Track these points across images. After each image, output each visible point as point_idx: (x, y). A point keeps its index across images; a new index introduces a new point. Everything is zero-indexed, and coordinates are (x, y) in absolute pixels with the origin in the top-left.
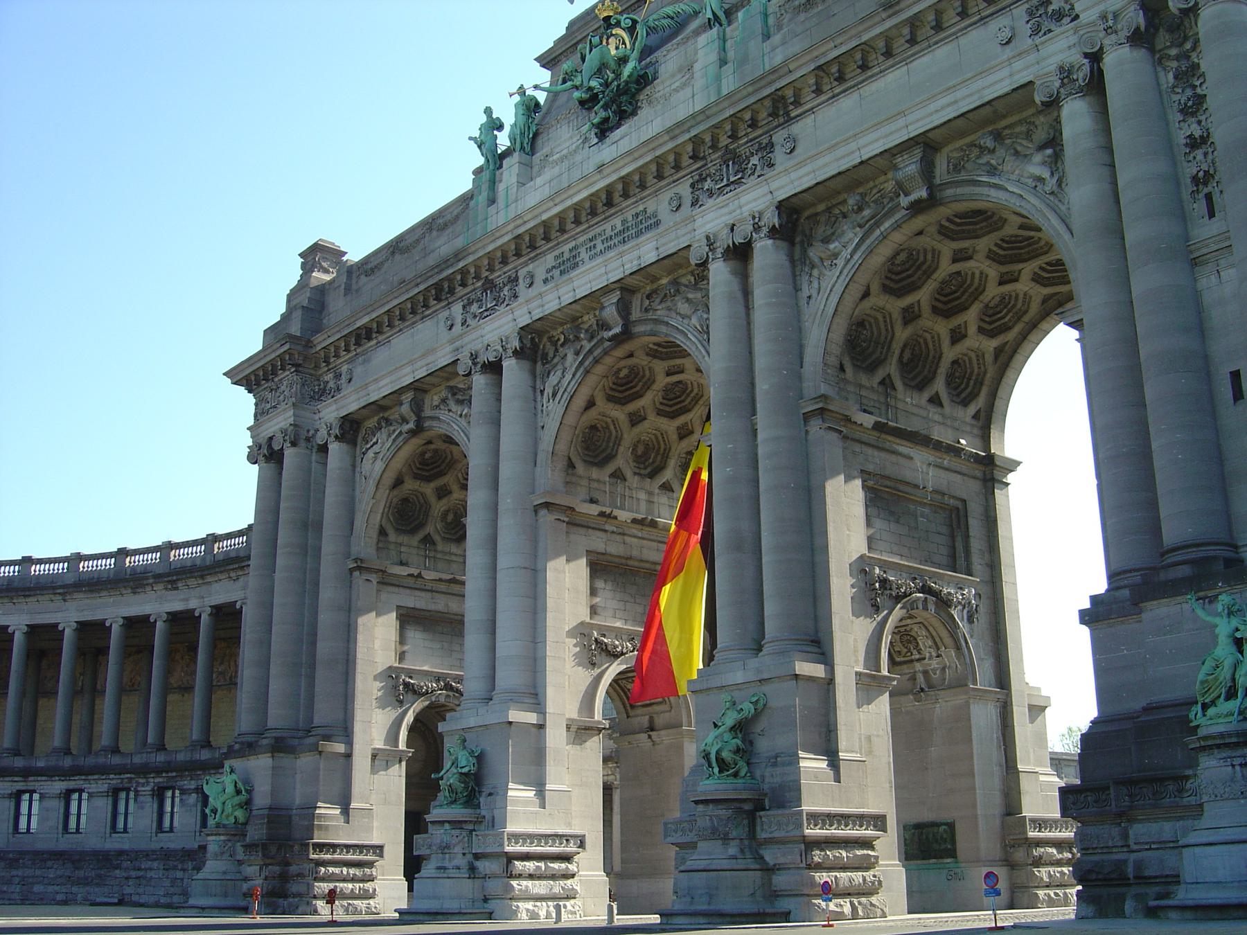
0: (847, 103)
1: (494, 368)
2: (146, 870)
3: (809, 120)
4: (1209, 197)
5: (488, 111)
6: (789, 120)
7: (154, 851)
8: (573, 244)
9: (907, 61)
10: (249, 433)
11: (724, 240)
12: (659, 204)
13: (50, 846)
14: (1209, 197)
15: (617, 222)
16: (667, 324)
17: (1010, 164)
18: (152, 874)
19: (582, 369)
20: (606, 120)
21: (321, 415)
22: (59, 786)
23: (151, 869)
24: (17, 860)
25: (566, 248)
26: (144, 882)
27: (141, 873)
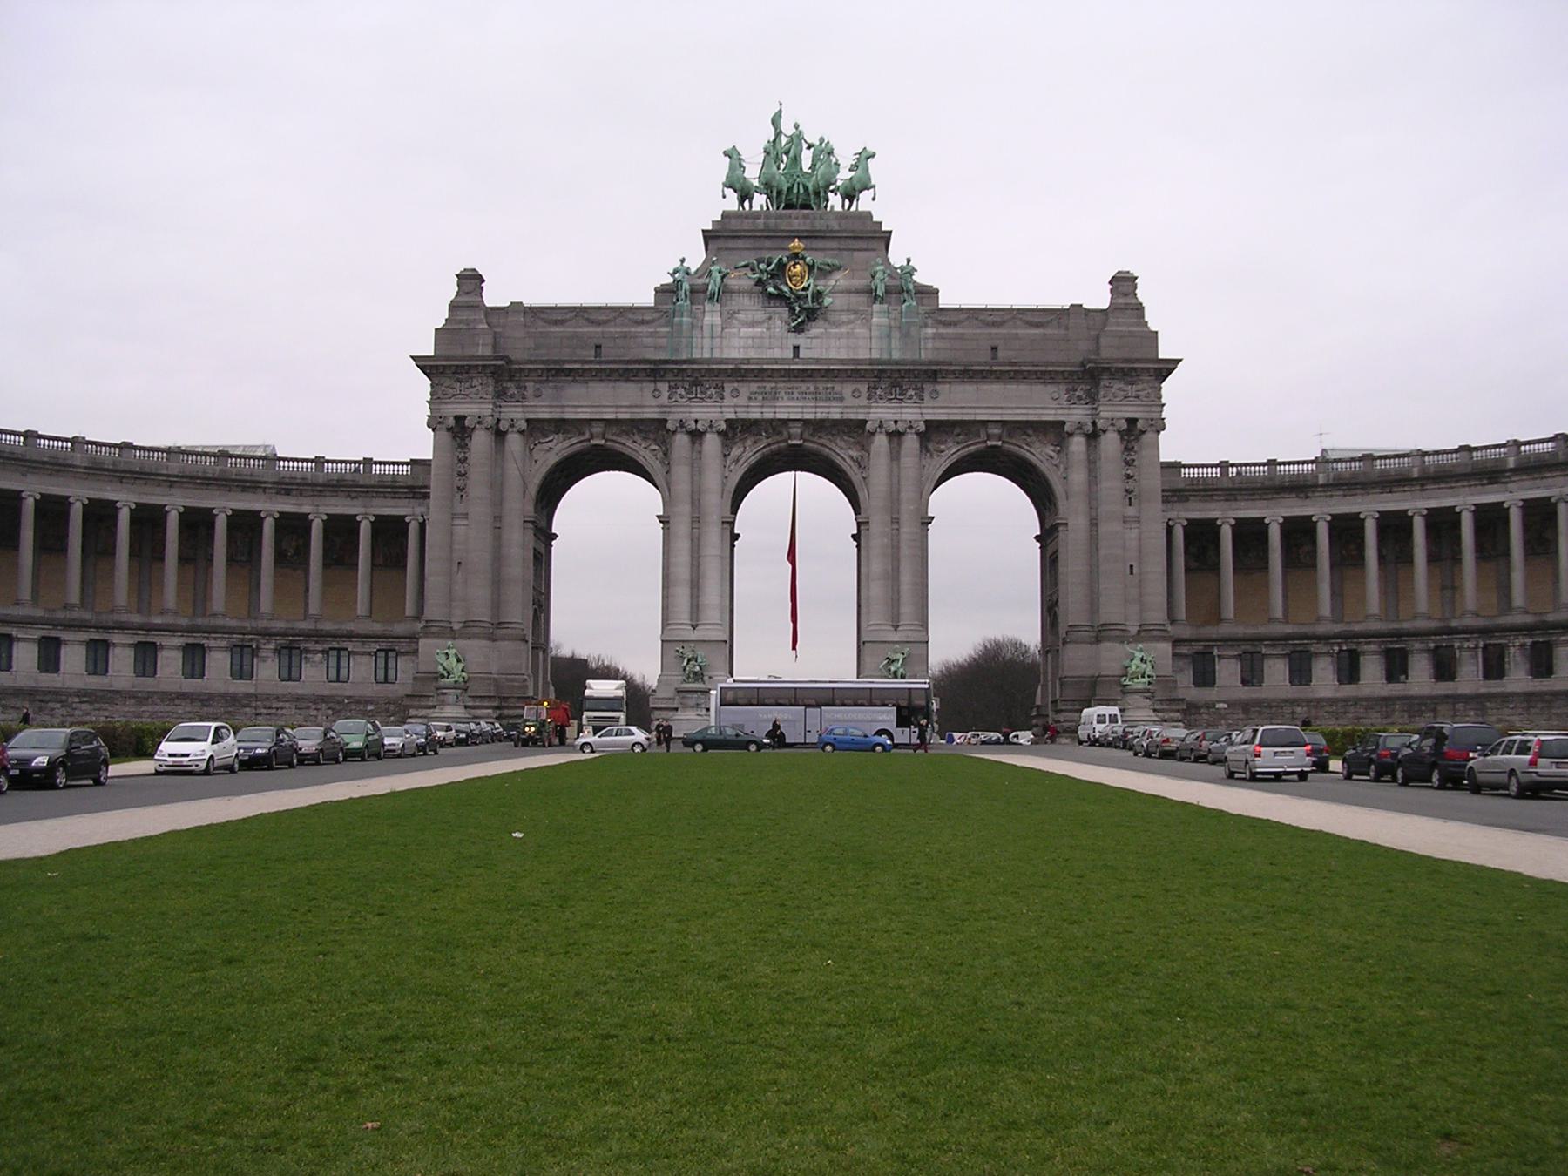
1: (696, 436)
2: (277, 709)
3: (947, 386)
4: (1130, 499)
5: (683, 261)
6: (935, 381)
7: (284, 696)
8: (774, 385)
9: (1005, 383)
11: (892, 427)
12: (847, 389)
13: (176, 688)
14: (1130, 499)
16: (831, 449)
17: (1037, 444)
18: (284, 711)
20: (803, 322)
21: (502, 410)
22: (178, 641)
23: (282, 708)
24: (147, 699)
25: (769, 386)
26: (273, 717)
27: (270, 711)
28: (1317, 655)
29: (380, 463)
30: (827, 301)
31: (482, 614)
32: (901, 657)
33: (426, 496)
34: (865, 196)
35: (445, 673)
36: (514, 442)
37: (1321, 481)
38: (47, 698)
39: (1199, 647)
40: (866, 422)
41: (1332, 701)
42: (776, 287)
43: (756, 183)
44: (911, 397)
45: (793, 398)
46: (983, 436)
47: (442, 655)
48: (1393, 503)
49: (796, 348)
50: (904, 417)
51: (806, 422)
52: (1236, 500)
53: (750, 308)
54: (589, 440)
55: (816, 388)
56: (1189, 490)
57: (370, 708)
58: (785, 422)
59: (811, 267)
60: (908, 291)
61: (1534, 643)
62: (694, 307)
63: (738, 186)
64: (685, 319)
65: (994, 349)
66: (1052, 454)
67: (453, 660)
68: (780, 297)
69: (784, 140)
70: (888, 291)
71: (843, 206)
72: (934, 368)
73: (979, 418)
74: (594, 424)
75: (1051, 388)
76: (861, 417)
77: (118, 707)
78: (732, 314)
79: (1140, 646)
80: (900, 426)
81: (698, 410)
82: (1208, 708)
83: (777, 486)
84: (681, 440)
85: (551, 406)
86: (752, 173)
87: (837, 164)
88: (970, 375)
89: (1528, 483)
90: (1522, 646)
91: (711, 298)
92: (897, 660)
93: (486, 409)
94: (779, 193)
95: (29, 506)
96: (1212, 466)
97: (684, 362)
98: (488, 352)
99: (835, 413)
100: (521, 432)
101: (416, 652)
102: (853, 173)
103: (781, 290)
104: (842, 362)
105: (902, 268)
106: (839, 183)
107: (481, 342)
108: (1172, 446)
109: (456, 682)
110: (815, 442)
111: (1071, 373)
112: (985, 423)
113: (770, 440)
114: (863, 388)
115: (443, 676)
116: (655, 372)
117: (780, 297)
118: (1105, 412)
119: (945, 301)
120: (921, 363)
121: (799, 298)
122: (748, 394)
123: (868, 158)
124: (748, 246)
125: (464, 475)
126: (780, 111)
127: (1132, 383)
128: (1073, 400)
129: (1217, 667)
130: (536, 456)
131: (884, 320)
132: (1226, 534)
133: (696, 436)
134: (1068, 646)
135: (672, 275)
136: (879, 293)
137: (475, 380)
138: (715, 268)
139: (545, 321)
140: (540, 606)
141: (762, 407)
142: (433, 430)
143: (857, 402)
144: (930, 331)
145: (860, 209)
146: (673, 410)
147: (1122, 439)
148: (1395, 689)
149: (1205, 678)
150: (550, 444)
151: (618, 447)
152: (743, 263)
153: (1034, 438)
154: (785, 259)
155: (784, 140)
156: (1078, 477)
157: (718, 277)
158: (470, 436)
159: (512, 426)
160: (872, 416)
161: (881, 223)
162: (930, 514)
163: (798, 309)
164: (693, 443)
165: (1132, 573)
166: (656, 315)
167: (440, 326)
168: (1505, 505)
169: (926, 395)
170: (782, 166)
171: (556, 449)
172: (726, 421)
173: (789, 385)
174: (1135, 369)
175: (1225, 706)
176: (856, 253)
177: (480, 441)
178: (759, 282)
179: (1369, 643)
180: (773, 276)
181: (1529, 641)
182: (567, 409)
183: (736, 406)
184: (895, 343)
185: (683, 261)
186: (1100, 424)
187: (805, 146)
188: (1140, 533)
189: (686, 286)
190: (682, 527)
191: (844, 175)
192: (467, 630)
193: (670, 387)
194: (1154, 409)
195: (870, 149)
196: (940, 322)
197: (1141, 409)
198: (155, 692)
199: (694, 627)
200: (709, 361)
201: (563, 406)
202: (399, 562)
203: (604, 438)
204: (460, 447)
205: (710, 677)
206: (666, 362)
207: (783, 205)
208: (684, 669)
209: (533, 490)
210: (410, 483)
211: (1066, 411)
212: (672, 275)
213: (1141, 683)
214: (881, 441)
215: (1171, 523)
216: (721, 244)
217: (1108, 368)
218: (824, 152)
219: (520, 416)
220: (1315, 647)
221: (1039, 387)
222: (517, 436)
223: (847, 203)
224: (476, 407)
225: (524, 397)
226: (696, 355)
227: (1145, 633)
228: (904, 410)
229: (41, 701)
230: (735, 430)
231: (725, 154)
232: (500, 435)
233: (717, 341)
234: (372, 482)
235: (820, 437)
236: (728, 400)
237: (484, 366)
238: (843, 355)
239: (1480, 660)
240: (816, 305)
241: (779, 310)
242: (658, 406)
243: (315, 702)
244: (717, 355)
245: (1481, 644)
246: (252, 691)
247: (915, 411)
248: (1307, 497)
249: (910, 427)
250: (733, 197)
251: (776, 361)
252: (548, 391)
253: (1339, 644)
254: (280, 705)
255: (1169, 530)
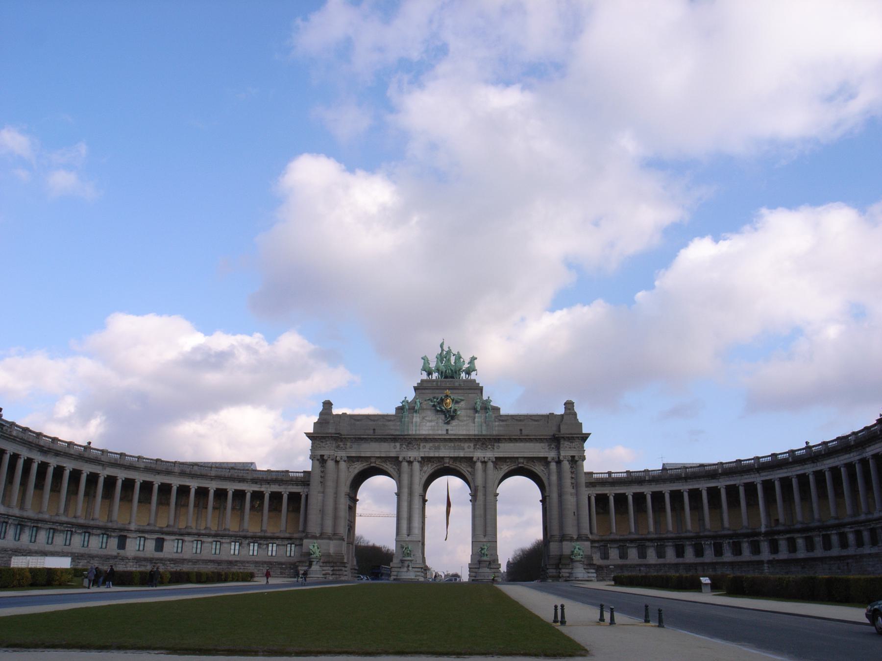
0: (512, 445)
1: (410, 463)
3: (503, 444)
5: (406, 398)
6: (499, 442)
7: (250, 561)
10: (310, 451)
11: (483, 460)
12: (466, 445)
15: (453, 445)
17: (537, 466)
18: (250, 568)
19: (433, 470)
20: (450, 420)
22: (210, 540)
23: (249, 566)
25: (437, 444)
27: (245, 567)
28: (648, 546)
29: (292, 472)
30: (459, 413)
31: (329, 530)
32: (486, 547)
33: (308, 485)
34: (473, 373)
35: (313, 553)
36: (343, 465)
37: (647, 479)
38: (157, 562)
39: (602, 544)
40: (472, 458)
41: (655, 565)
42: (440, 408)
43: (433, 369)
44: (489, 448)
45: (446, 449)
46: (517, 463)
47: (314, 547)
48: (676, 487)
49: (447, 430)
50: (487, 456)
51: (451, 458)
52: (614, 486)
53: (430, 415)
54: (370, 464)
55: (454, 445)
56: (596, 483)
57: (284, 566)
58: (443, 458)
59: (453, 400)
60: (489, 409)
61: (733, 542)
62: (410, 415)
63: (427, 370)
64: (406, 419)
65: (521, 430)
66: (543, 469)
67: (316, 548)
68: (442, 411)
69: (445, 353)
70: (481, 409)
71: (466, 377)
72: (498, 437)
73: (515, 456)
74: (372, 458)
75: (542, 444)
76: (471, 456)
77: (184, 566)
78: (423, 418)
79: (578, 543)
80: (486, 459)
81: (411, 453)
82: (606, 568)
83: (441, 483)
84: (405, 464)
85: (356, 452)
86: (433, 365)
87: (464, 361)
88: (511, 440)
89: (727, 479)
90: (729, 543)
91: (416, 412)
92: (485, 549)
93: (332, 453)
94: (442, 372)
95: (156, 487)
96: (605, 473)
97: (405, 435)
98: (333, 431)
99: (462, 455)
100: (345, 461)
101: (301, 545)
102: (469, 365)
103: (442, 409)
104: (463, 435)
105: (486, 400)
106: (464, 369)
107: (330, 428)
108: (588, 466)
109: (317, 556)
110: (454, 465)
111: (549, 439)
112: (517, 458)
113: (438, 465)
114: (472, 445)
115: (312, 554)
116: (394, 439)
117: (442, 411)
118: (563, 453)
119: (502, 412)
120: (494, 436)
121: (448, 411)
122: (429, 447)
123: (474, 360)
124: (430, 392)
125: (323, 477)
126: (443, 342)
127: (572, 442)
128: (550, 448)
129: (609, 551)
130: (350, 470)
131: (480, 420)
132: (612, 499)
133: (410, 463)
134: (551, 543)
135: (402, 403)
136: (478, 410)
137: (328, 443)
138: (418, 400)
139: (355, 420)
140: (351, 527)
141: (434, 452)
142: (312, 460)
143: (469, 450)
144: (497, 423)
145: (472, 378)
146: (401, 453)
147: (569, 463)
148: (680, 560)
149: (605, 556)
150: (356, 466)
151: (381, 467)
152: (428, 399)
153: (536, 464)
154: (443, 397)
155: (445, 353)
156: (554, 478)
157: (419, 404)
158: (325, 463)
159: (341, 459)
160: (475, 455)
161: (479, 384)
162: (497, 492)
163: (448, 416)
164: (409, 465)
165: (574, 514)
166: (396, 418)
167: (315, 421)
168: (719, 487)
169: (495, 448)
170: (444, 362)
171: (358, 467)
172: (422, 457)
173: (444, 444)
174: (573, 437)
175: (613, 567)
176: (470, 395)
177: (331, 464)
178: (434, 406)
179: (669, 542)
180: (439, 403)
181: (731, 541)
182: (362, 453)
183: (424, 452)
184: (484, 428)
185: (406, 398)
186: (561, 458)
187: (452, 355)
188: (577, 499)
189: (407, 407)
190: (405, 497)
191: (466, 366)
192: (322, 536)
193: (400, 445)
194: (581, 452)
195: (475, 356)
196: (500, 420)
197: (576, 452)
198: (200, 560)
199: (408, 535)
200: (414, 435)
201: (361, 452)
202: (297, 510)
203: (375, 463)
204: (322, 466)
205: (414, 555)
206: (399, 435)
207: (443, 377)
208: (404, 552)
209: (349, 483)
210: (303, 480)
211: (547, 453)
212: (402, 403)
213: (578, 558)
214: (479, 465)
215: (590, 495)
216: (420, 391)
217: (563, 437)
218: (458, 357)
219: (344, 455)
220: (648, 544)
221: (538, 444)
222: (343, 462)
223: (467, 376)
224: (327, 451)
225: (346, 448)
226: (410, 433)
227: (580, 538)
228: (487, 453)
229: (155, 563)
230: (425, 460)
231: (422, 358)
232: (337, 462)
233: (418, 428)
234: (288, 479)
235: (456, 463)
236: (421, 450)
237: (331, 437)
238: (464, 433)
239: (713, 549)
240: (454, 414)
241: (441, 416)
242: (396, 452)
243: (262, 564)
244: (418, 432)
245: (713, 542)
246: (238, 559)
247: (491, 453)
248: (642, 485)
249: (490, 460)
250: (425, 373)
251: (439, 435)
252: (355, 446)
253: (657, 543)
254: (248, 565)
255: (589, 498)
